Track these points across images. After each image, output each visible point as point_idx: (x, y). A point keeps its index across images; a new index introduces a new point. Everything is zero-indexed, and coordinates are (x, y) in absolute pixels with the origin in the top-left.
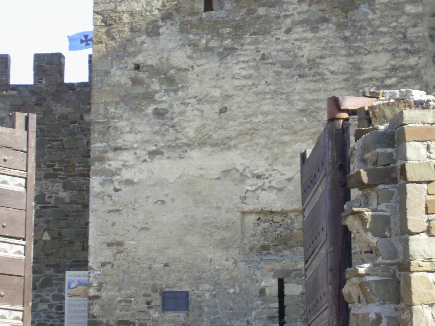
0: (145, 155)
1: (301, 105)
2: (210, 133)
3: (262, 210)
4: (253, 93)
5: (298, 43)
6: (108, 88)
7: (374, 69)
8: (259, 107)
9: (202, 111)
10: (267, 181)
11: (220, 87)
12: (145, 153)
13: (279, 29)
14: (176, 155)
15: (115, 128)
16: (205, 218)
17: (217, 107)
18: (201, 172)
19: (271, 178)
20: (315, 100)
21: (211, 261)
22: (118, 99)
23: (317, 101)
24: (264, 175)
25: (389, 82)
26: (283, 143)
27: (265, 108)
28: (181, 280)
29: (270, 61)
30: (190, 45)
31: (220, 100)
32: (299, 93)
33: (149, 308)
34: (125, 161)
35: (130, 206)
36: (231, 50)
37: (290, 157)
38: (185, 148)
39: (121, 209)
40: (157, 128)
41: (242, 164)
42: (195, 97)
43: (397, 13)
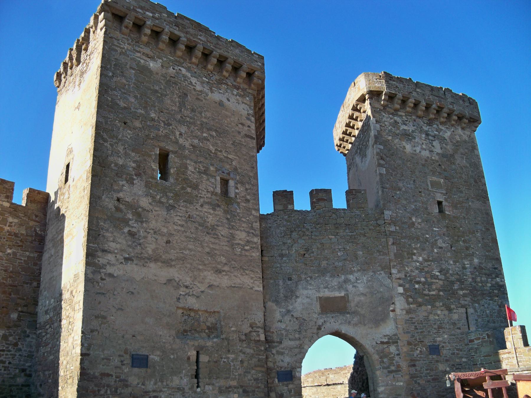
0: (122, 259)
1: (207, 250)
2: (161, 254)
3: (188, 307)
4: (184, 236)
5: (206, 214)
6: (100, 208)
7: (240, 239)
8: (187, 245)
9: (157, 239)
10: (191, 290)
11: (167, 227)
12: (122, 258)
13: (198, 203)
14: (141, 264)
15: (103, 236)
16: (157, 308)
17: (165, 239)
18: (156, 278)
19: (193, 289)
20: (214, 249)
21: (160, 336)
22: (106, 217)
23: (215, 249)
24: (190, 287)
25: (247, 248)
26: (199, 269)
27: (190, 247)
28: (143, 347)
29: (193, 220)
30: (151, 197)
31: (167, 235)
32: (207, 243)
33: (122, 365)
34: (109, 261)
35: (111, 292)
36: (173, 207)
37: (203, 279)
38: (146, 260)
39: (105, 293)
40: (130, 243)
41: (178, 277)
42: (153, 230)
43: (249, 213)
